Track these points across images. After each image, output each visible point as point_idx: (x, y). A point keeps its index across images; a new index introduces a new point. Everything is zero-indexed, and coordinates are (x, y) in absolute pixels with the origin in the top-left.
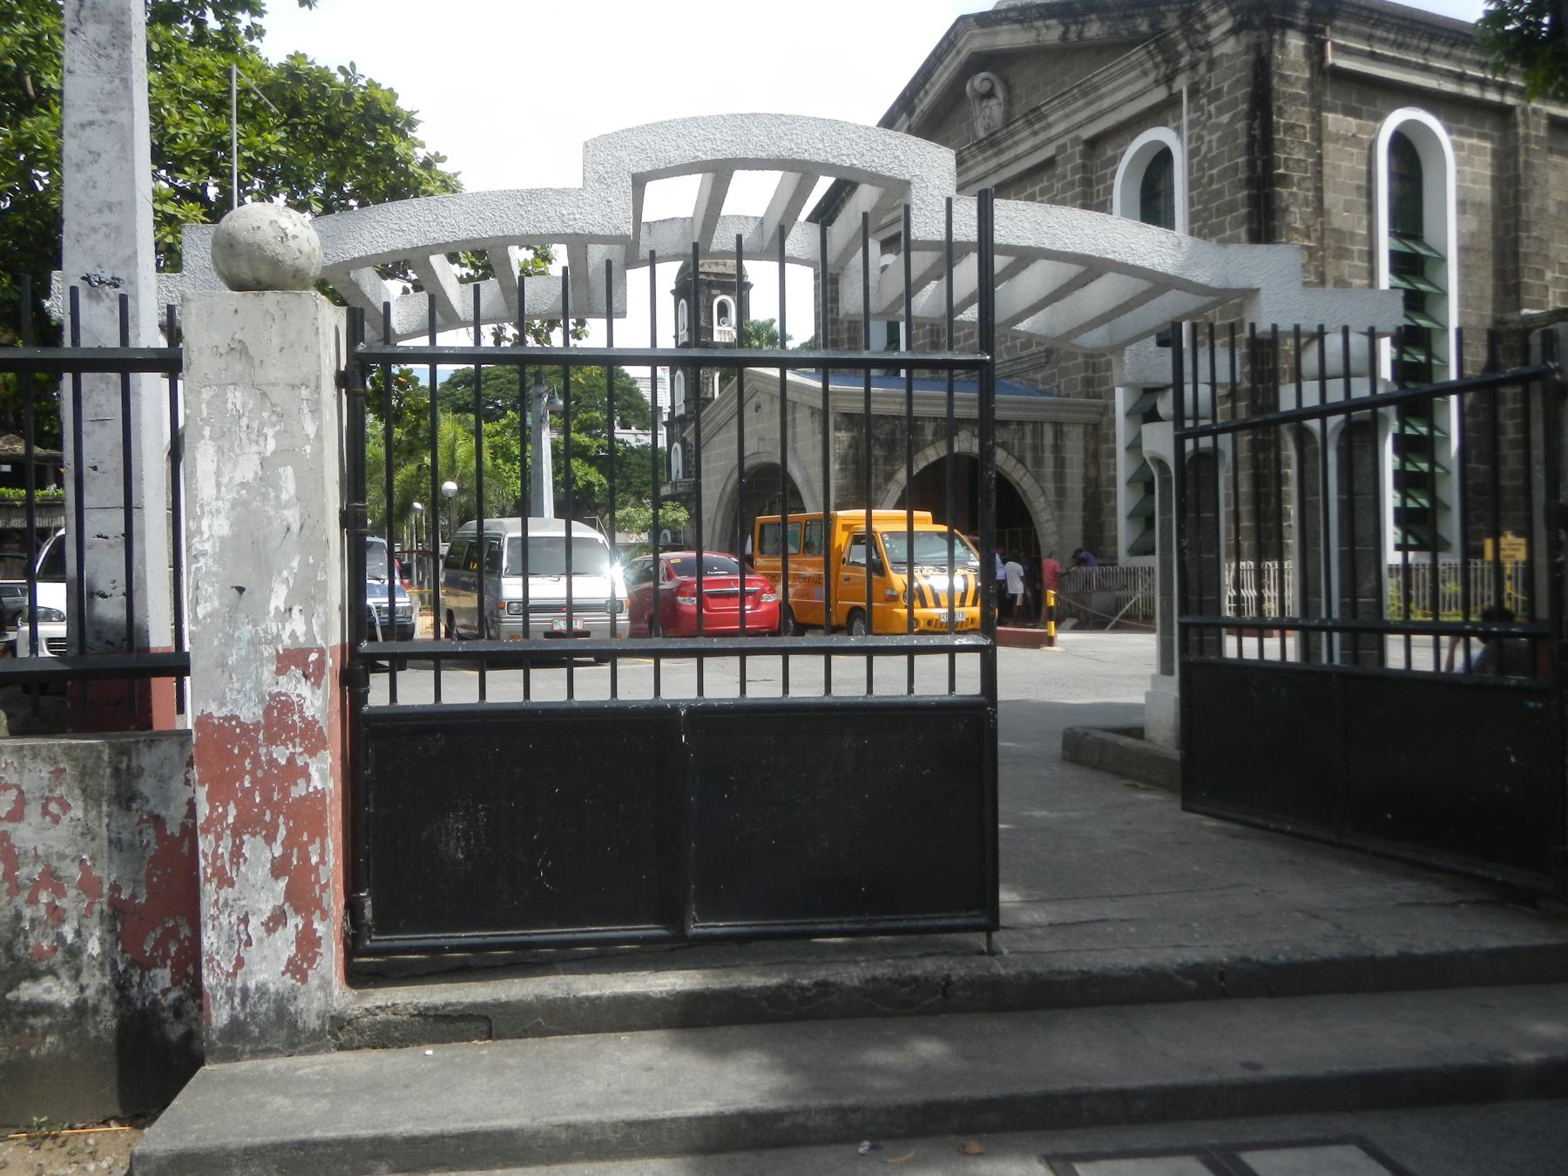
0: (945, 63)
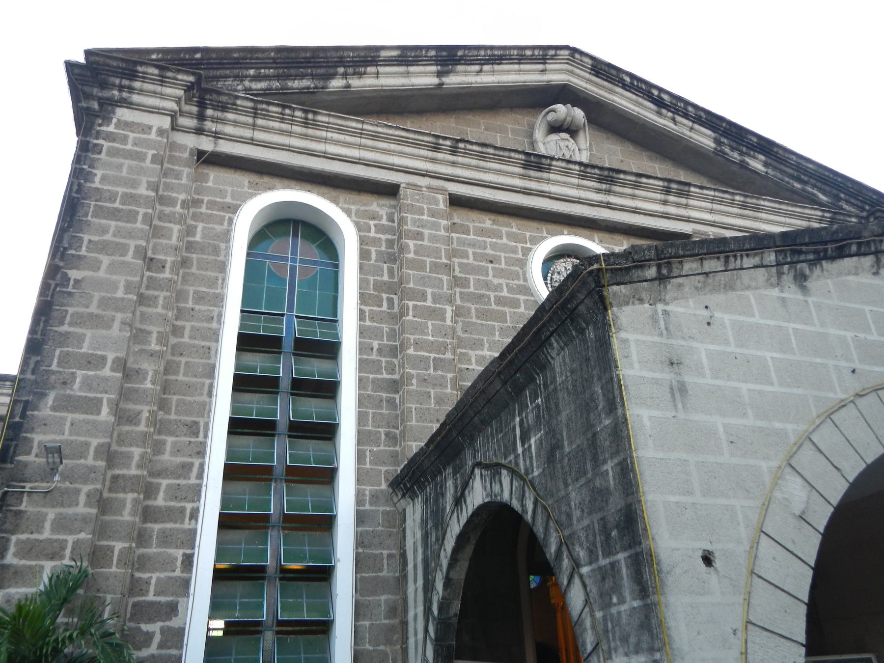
0: (523, 67)
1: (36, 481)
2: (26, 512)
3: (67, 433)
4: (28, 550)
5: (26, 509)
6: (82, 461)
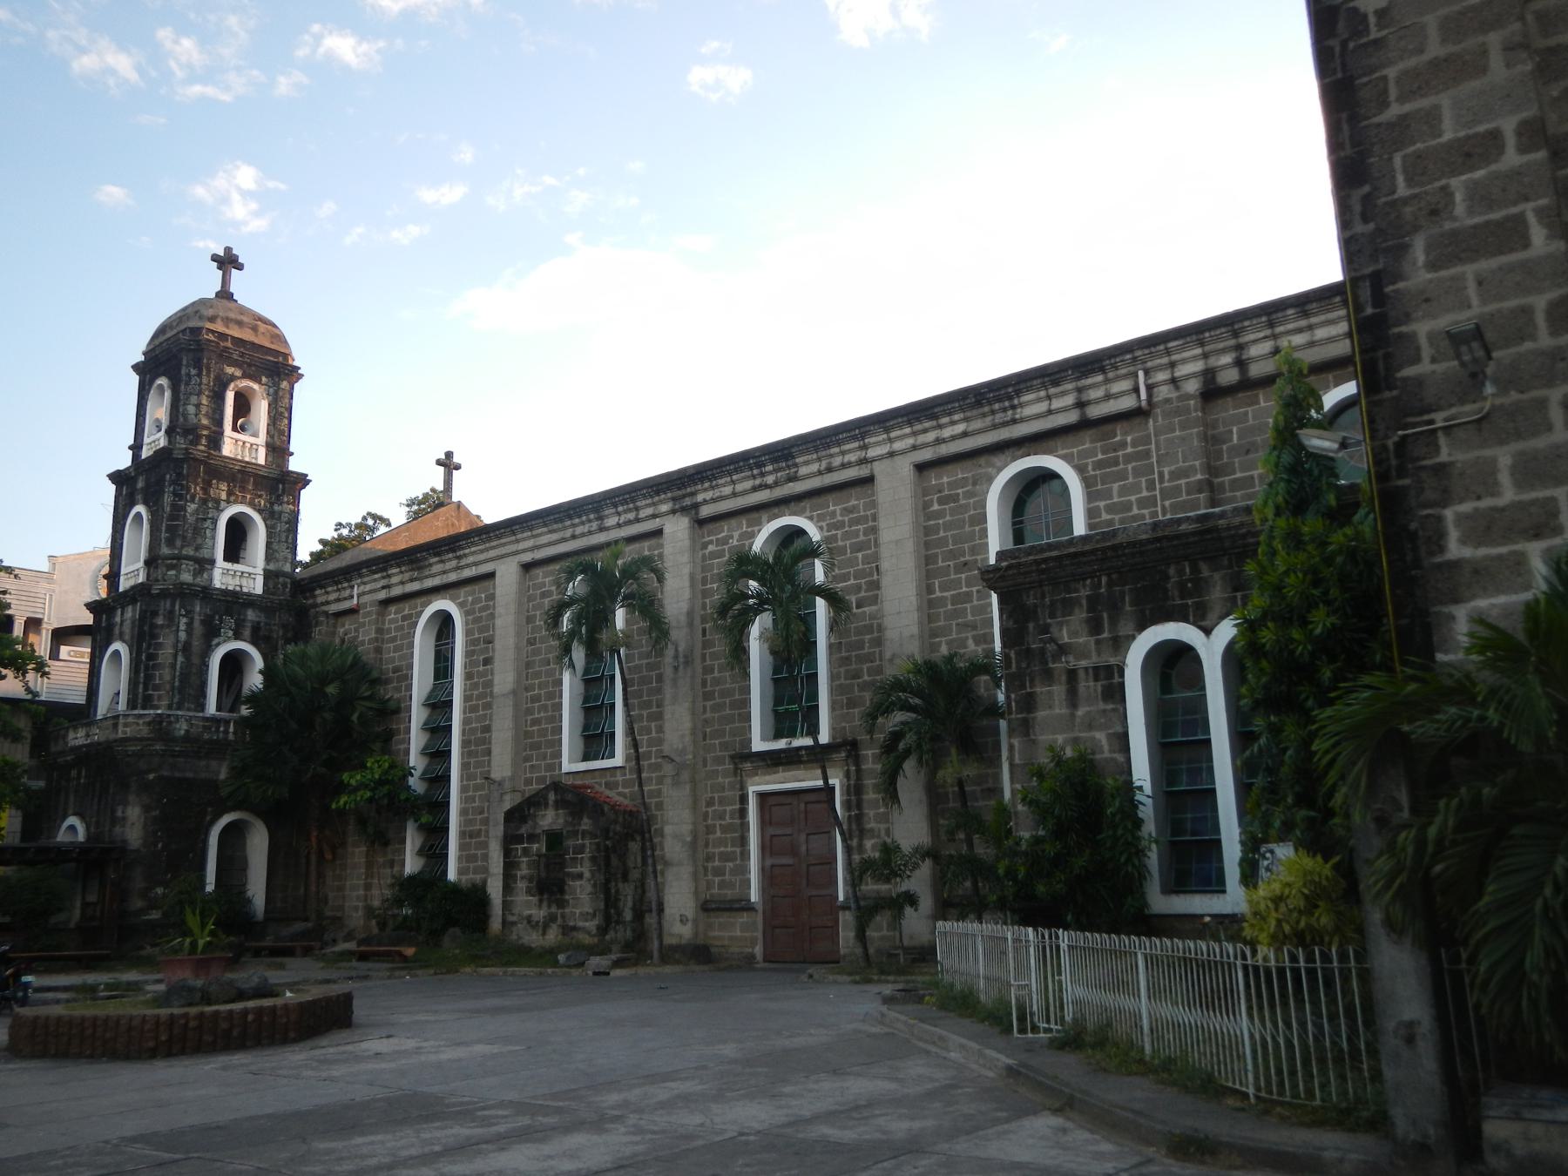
1: (1451, 406)
2: (1452, 464)
3: (1475, 301)
4: (1483, 528)
5: (1452, 459)
6: (1528, 345)
